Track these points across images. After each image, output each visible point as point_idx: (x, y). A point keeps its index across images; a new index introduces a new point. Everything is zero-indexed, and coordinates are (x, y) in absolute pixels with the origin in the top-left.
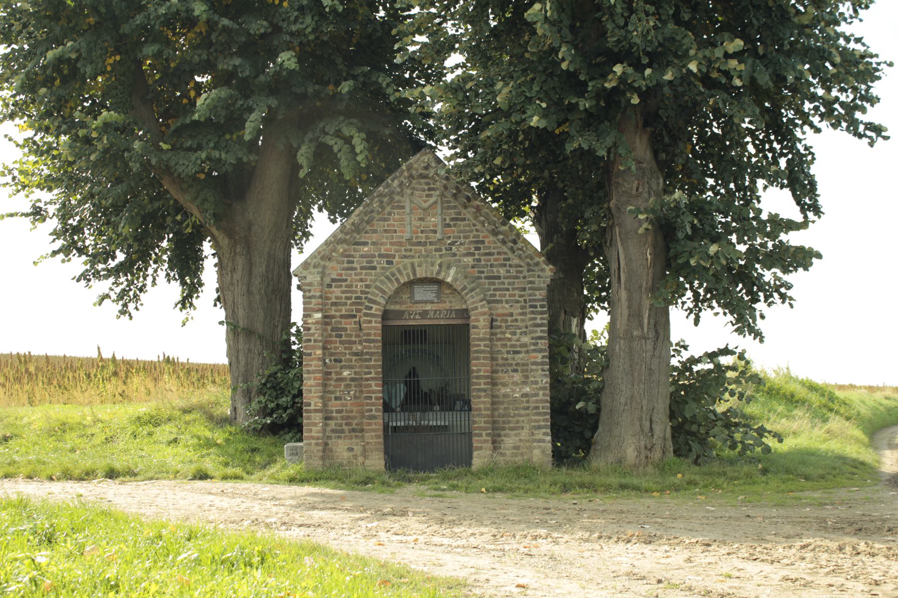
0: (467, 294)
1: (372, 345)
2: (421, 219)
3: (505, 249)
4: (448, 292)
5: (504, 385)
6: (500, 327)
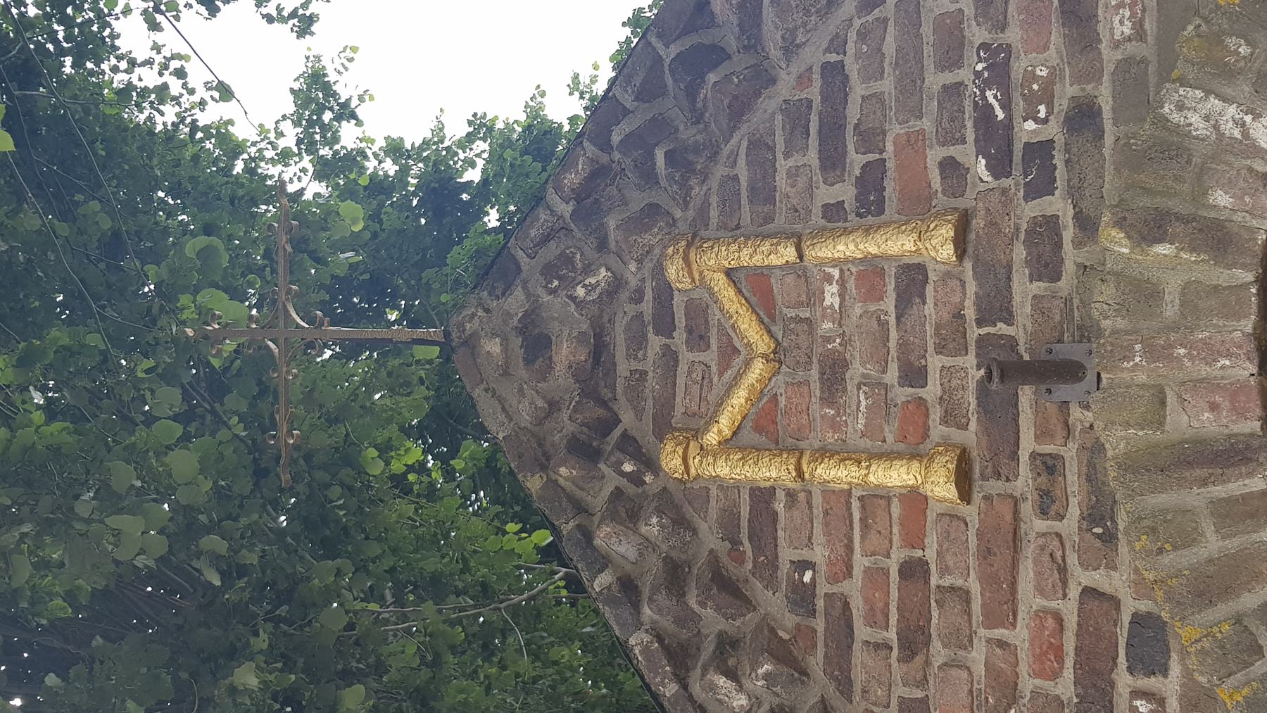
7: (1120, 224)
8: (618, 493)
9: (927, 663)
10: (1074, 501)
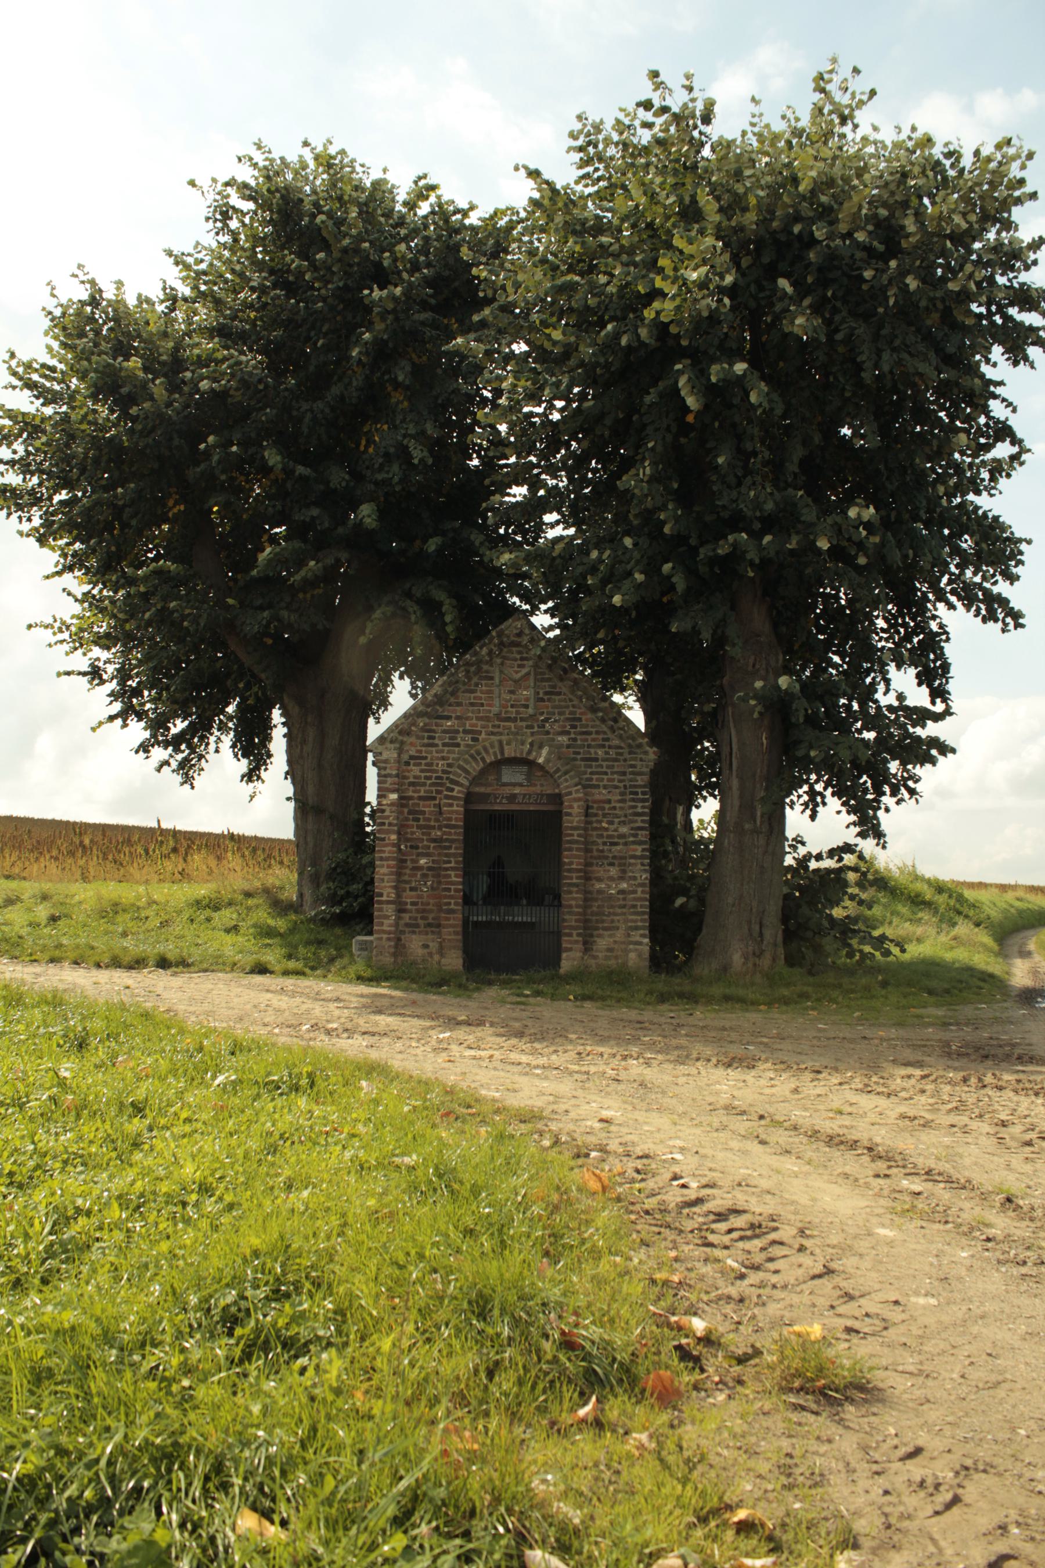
2: (512, 692)
3: (605, 729)
4: (539, 774)
5: (599, 880)
6: (596, 815)
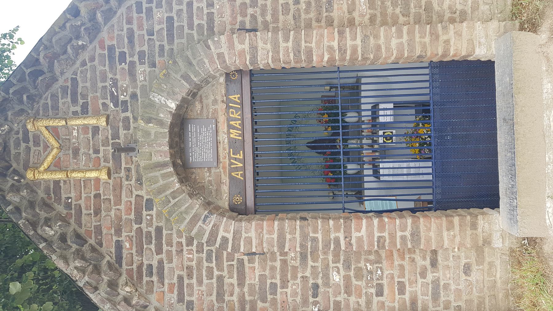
0: (197, 74)
1: (288, 236)
2: (76, 152)
3: (123, 10)
4: (198, 106)
6: (254, 17)
7: (142, 119)
8: (13, 185)
9: (101, 216)
10: (134, 177)
